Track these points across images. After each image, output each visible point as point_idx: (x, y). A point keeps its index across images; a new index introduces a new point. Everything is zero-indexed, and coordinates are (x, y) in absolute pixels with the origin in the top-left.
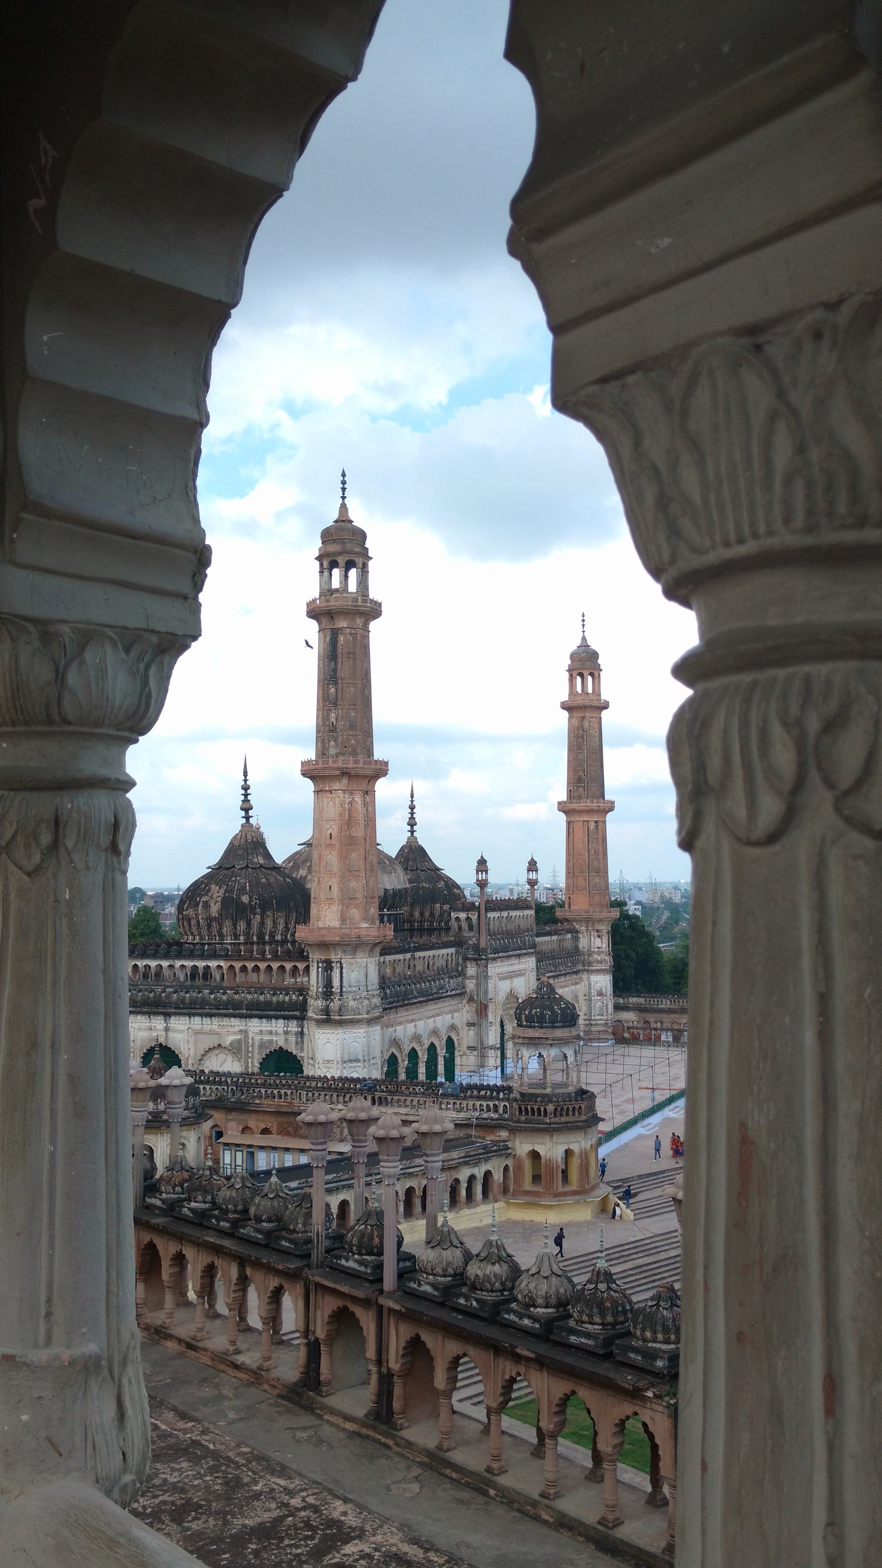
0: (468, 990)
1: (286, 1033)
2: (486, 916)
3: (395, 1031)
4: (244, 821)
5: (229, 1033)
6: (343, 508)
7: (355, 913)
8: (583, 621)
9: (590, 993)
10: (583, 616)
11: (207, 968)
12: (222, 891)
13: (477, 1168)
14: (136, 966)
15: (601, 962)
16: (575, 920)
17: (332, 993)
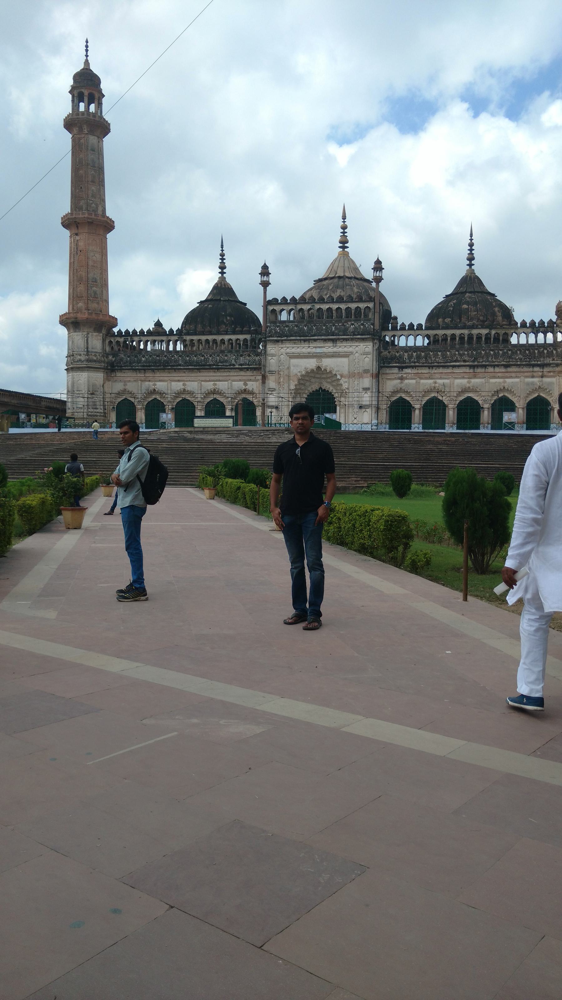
3: (155, 385)
4: (220, 275)
6: (87, 63)
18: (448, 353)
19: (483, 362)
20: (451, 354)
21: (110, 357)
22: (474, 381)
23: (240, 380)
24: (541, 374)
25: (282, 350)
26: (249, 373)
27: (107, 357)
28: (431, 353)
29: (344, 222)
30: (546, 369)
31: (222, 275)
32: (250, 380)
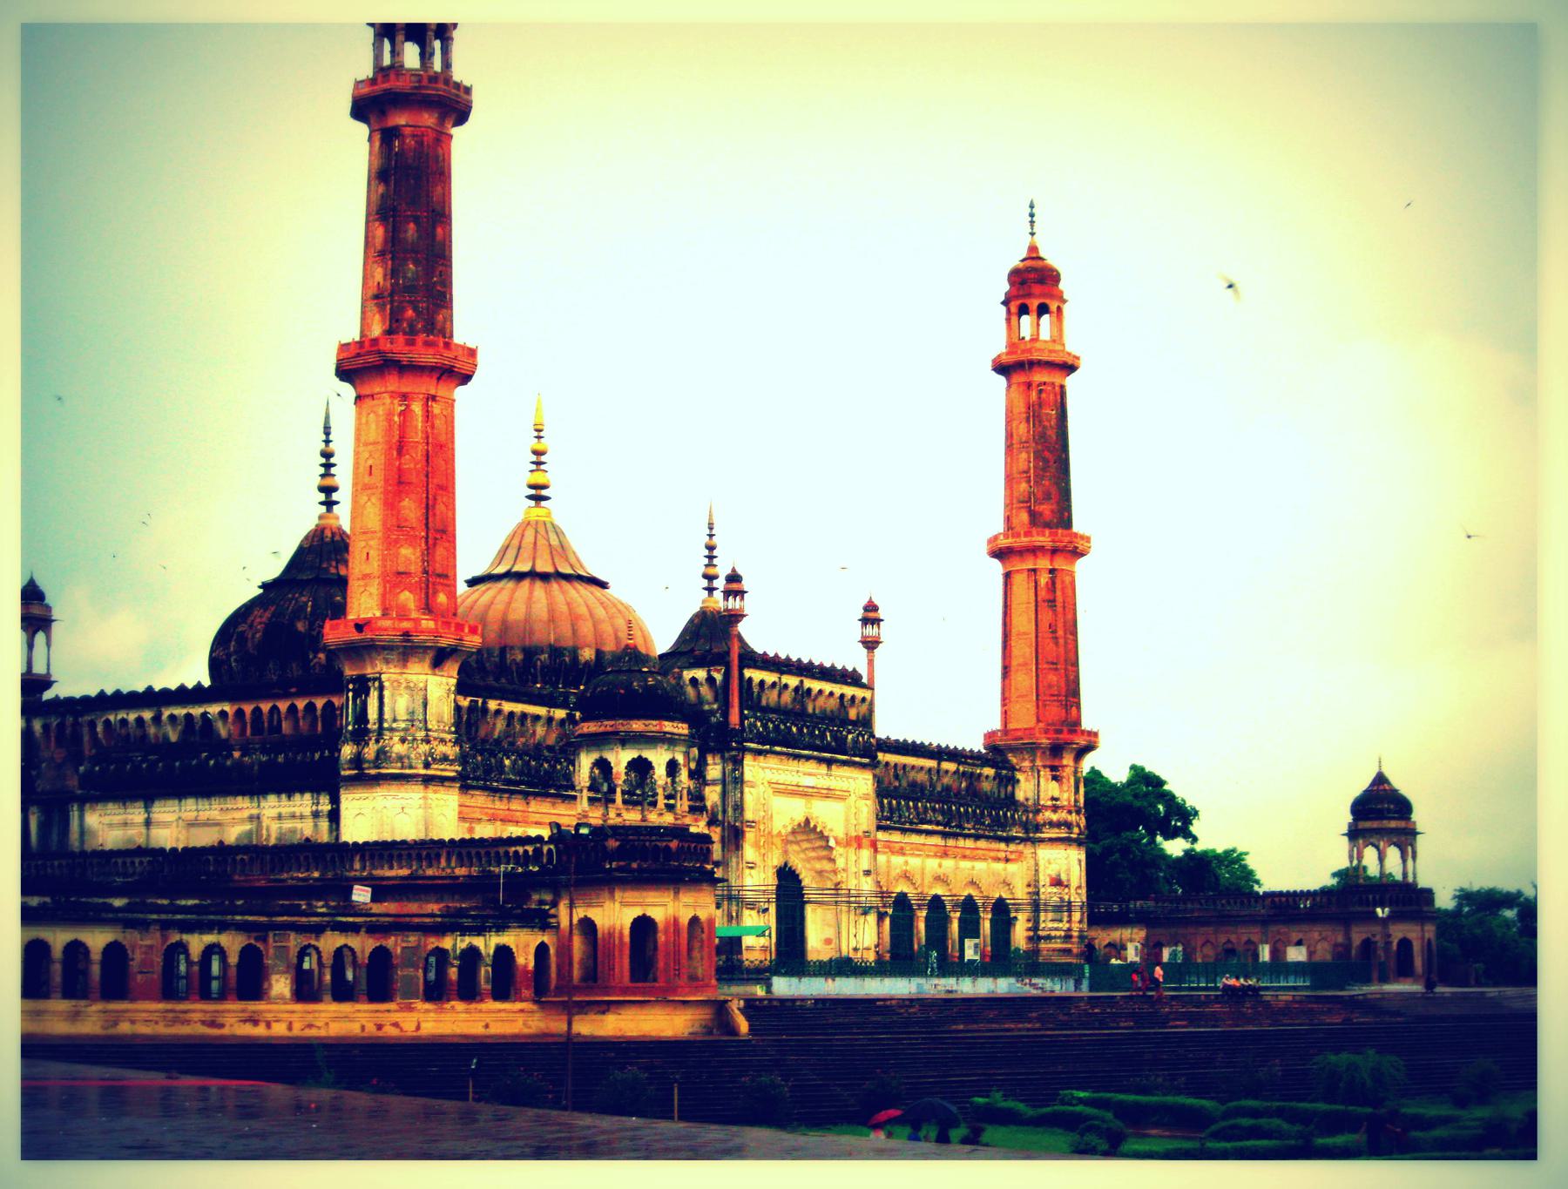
0: (709, 804)
1: (316, 815)
2: (741, 675)
4: (324, 509)
5: (234, 822)
7: (407, 598)
8: (1032, 215)
9: (1037, 881)
10: (1032, 207)
11: (204, 714)
12: (268, 614)
13: (481, 939)
14: (107, 722)
15: (1058, 825)
16: (1013, 750)
17: (367, 731)
30: (1012, 847)
31: (329, 510)
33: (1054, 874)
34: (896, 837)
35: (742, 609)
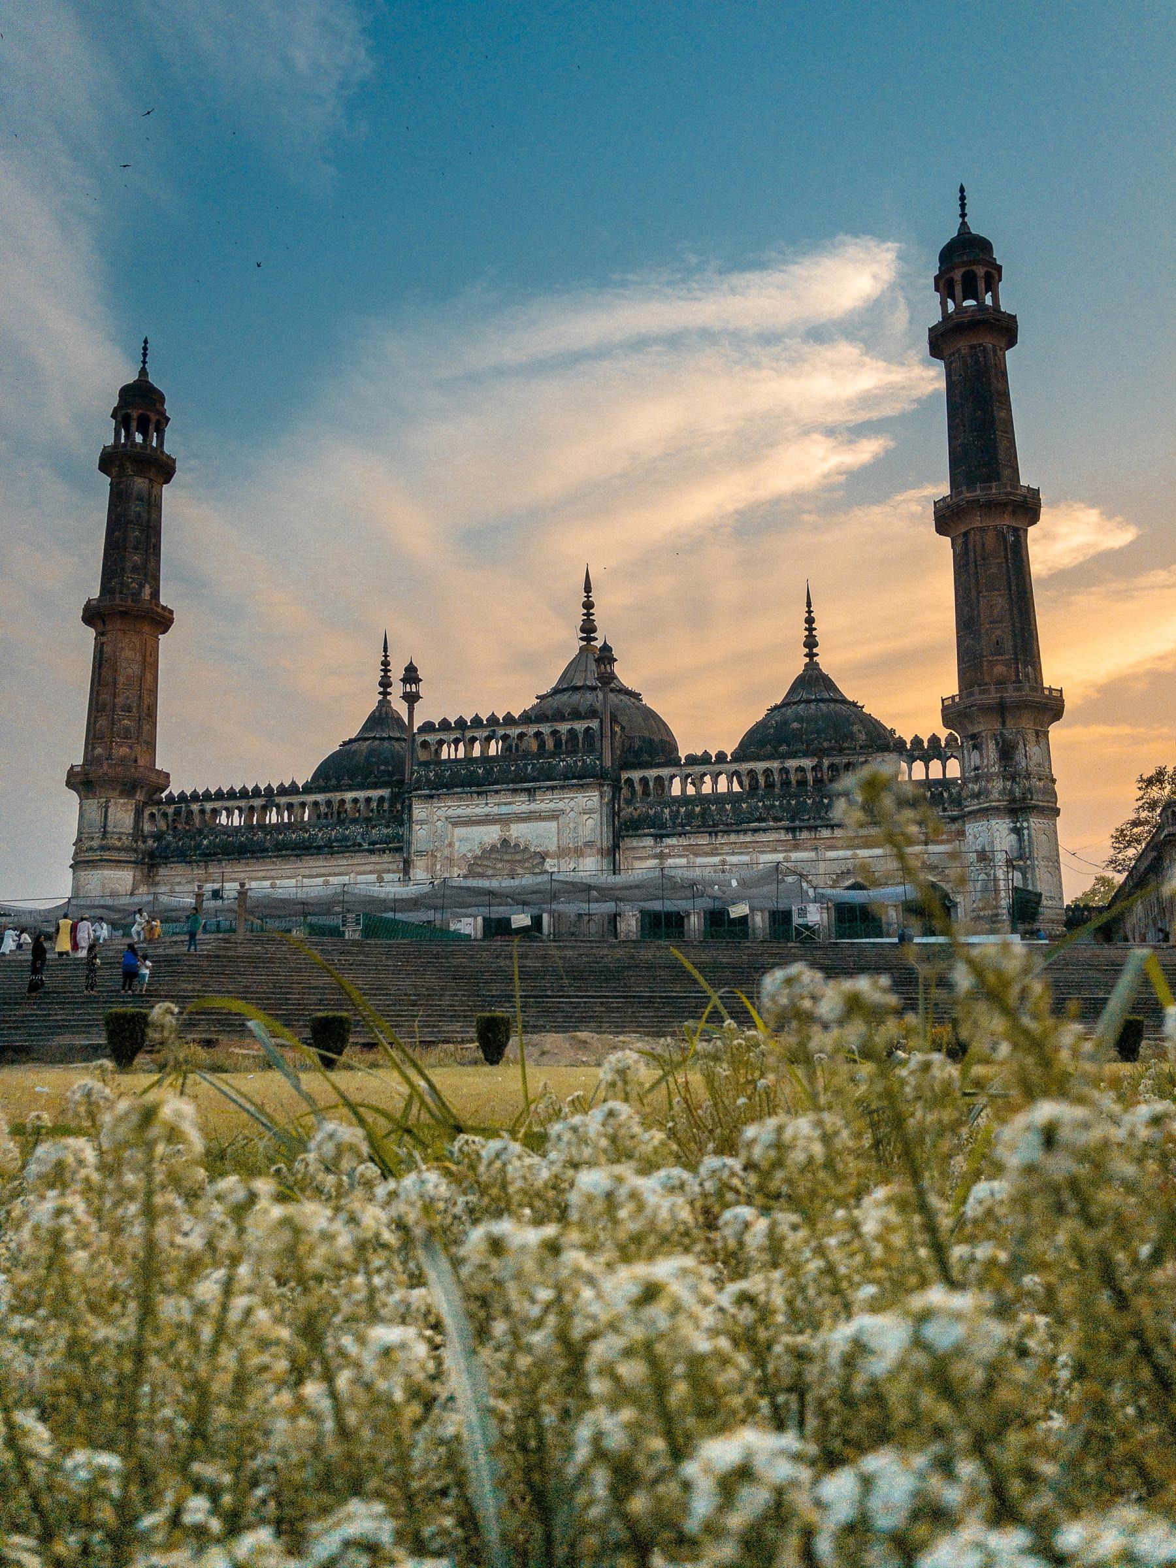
6: (143, 372)
10: (962, 190)
15: (976, 796)
18: (744, 806)
19: (808, 820)
20: (749, 806)
21: (150, 842)
22: (794, 856)
23: (371, 872)
24: (923, 838)
25: (439, 813)
26: (387, 857)
27: (144, 842)
28: (713, 808)
29: (588, 597)
32: (389, 871)
33: (979, 848)
34: (703, 840)
35: (417, 692)
